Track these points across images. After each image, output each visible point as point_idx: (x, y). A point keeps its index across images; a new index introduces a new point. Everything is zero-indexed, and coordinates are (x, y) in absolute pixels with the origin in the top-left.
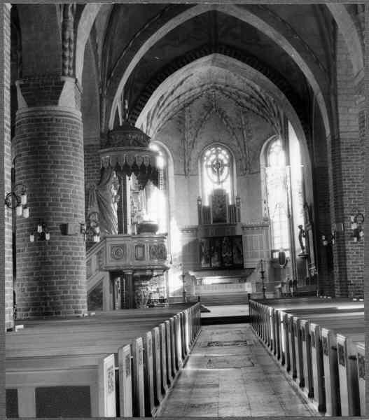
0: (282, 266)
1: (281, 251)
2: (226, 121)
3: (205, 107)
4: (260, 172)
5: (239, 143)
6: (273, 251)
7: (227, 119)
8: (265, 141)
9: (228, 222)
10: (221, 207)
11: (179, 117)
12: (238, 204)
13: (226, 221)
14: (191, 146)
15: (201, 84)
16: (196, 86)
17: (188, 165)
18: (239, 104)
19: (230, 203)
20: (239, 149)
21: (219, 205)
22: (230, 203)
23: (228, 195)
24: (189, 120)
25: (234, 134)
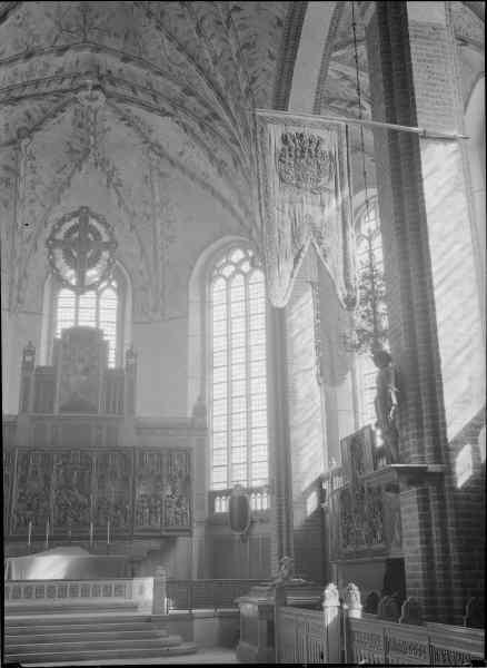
0: (237, 535)
1: (236, 494)
2: (117, 191)
3: (72, 151)
4: (186, 316)
5: (143, 251)
6: (214, 495)
7: (119, 188)
8: (203, 248)
9: (101, 412)
10: (86, 371)
11: (7, 168)
12: (131, 369)
13: (94, 410)
14: (28, 247)
15: (61, 43)
16: (44, 43)
17: (19, 288)
18: (151, 148)
19: (112, 366)
20: (142, 266)
21: (80, 367)
22: (112, 366)
23: (106, 344)
24: (29, 178)
25: (132, 227)
